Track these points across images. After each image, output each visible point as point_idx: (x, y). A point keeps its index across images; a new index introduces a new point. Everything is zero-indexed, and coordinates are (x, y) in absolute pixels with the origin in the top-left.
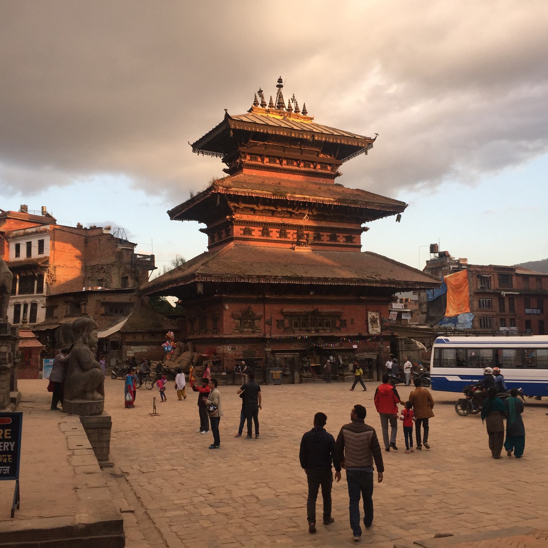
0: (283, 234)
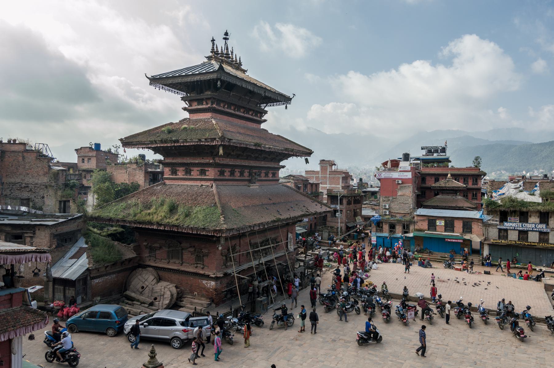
0: (242, 174)
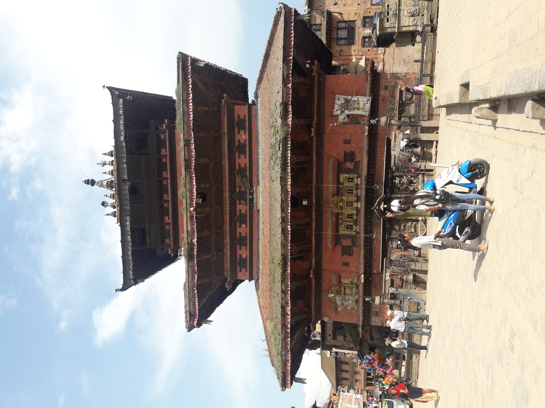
0: (242, 219)
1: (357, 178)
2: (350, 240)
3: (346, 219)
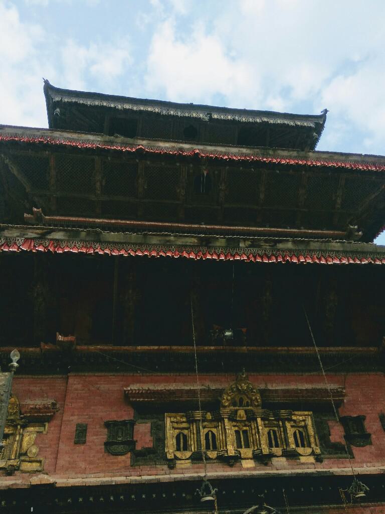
1: (313, 453)
2: (151, 445)
3: (203, 432)
